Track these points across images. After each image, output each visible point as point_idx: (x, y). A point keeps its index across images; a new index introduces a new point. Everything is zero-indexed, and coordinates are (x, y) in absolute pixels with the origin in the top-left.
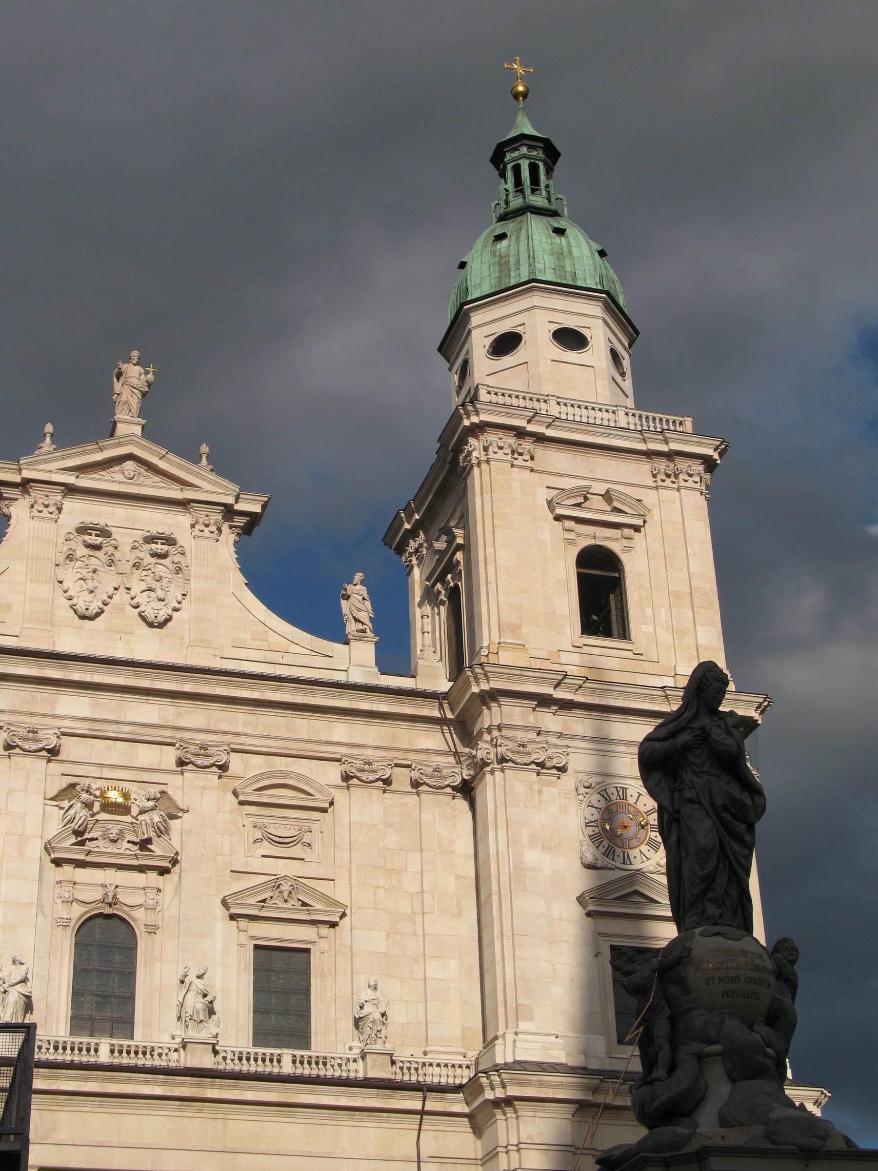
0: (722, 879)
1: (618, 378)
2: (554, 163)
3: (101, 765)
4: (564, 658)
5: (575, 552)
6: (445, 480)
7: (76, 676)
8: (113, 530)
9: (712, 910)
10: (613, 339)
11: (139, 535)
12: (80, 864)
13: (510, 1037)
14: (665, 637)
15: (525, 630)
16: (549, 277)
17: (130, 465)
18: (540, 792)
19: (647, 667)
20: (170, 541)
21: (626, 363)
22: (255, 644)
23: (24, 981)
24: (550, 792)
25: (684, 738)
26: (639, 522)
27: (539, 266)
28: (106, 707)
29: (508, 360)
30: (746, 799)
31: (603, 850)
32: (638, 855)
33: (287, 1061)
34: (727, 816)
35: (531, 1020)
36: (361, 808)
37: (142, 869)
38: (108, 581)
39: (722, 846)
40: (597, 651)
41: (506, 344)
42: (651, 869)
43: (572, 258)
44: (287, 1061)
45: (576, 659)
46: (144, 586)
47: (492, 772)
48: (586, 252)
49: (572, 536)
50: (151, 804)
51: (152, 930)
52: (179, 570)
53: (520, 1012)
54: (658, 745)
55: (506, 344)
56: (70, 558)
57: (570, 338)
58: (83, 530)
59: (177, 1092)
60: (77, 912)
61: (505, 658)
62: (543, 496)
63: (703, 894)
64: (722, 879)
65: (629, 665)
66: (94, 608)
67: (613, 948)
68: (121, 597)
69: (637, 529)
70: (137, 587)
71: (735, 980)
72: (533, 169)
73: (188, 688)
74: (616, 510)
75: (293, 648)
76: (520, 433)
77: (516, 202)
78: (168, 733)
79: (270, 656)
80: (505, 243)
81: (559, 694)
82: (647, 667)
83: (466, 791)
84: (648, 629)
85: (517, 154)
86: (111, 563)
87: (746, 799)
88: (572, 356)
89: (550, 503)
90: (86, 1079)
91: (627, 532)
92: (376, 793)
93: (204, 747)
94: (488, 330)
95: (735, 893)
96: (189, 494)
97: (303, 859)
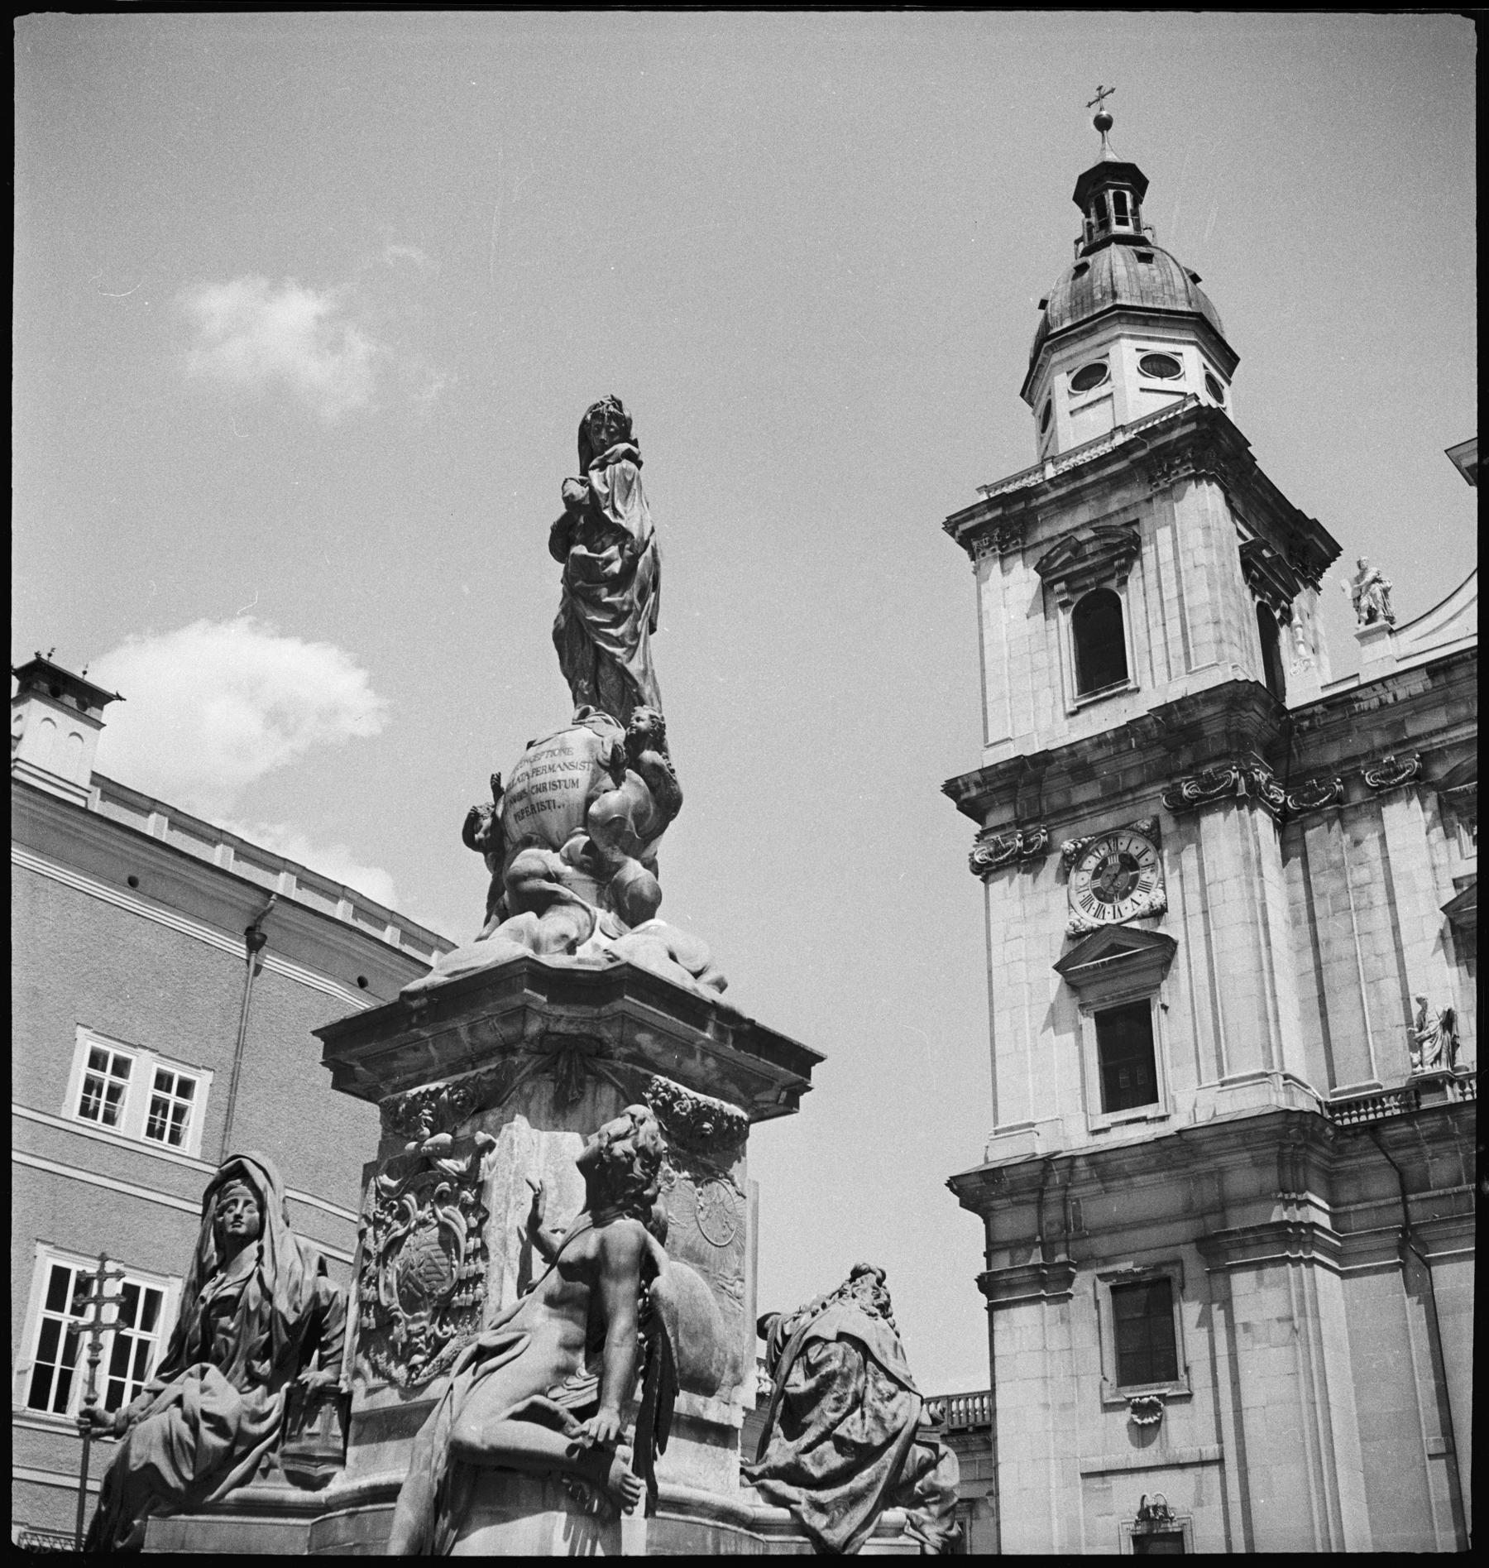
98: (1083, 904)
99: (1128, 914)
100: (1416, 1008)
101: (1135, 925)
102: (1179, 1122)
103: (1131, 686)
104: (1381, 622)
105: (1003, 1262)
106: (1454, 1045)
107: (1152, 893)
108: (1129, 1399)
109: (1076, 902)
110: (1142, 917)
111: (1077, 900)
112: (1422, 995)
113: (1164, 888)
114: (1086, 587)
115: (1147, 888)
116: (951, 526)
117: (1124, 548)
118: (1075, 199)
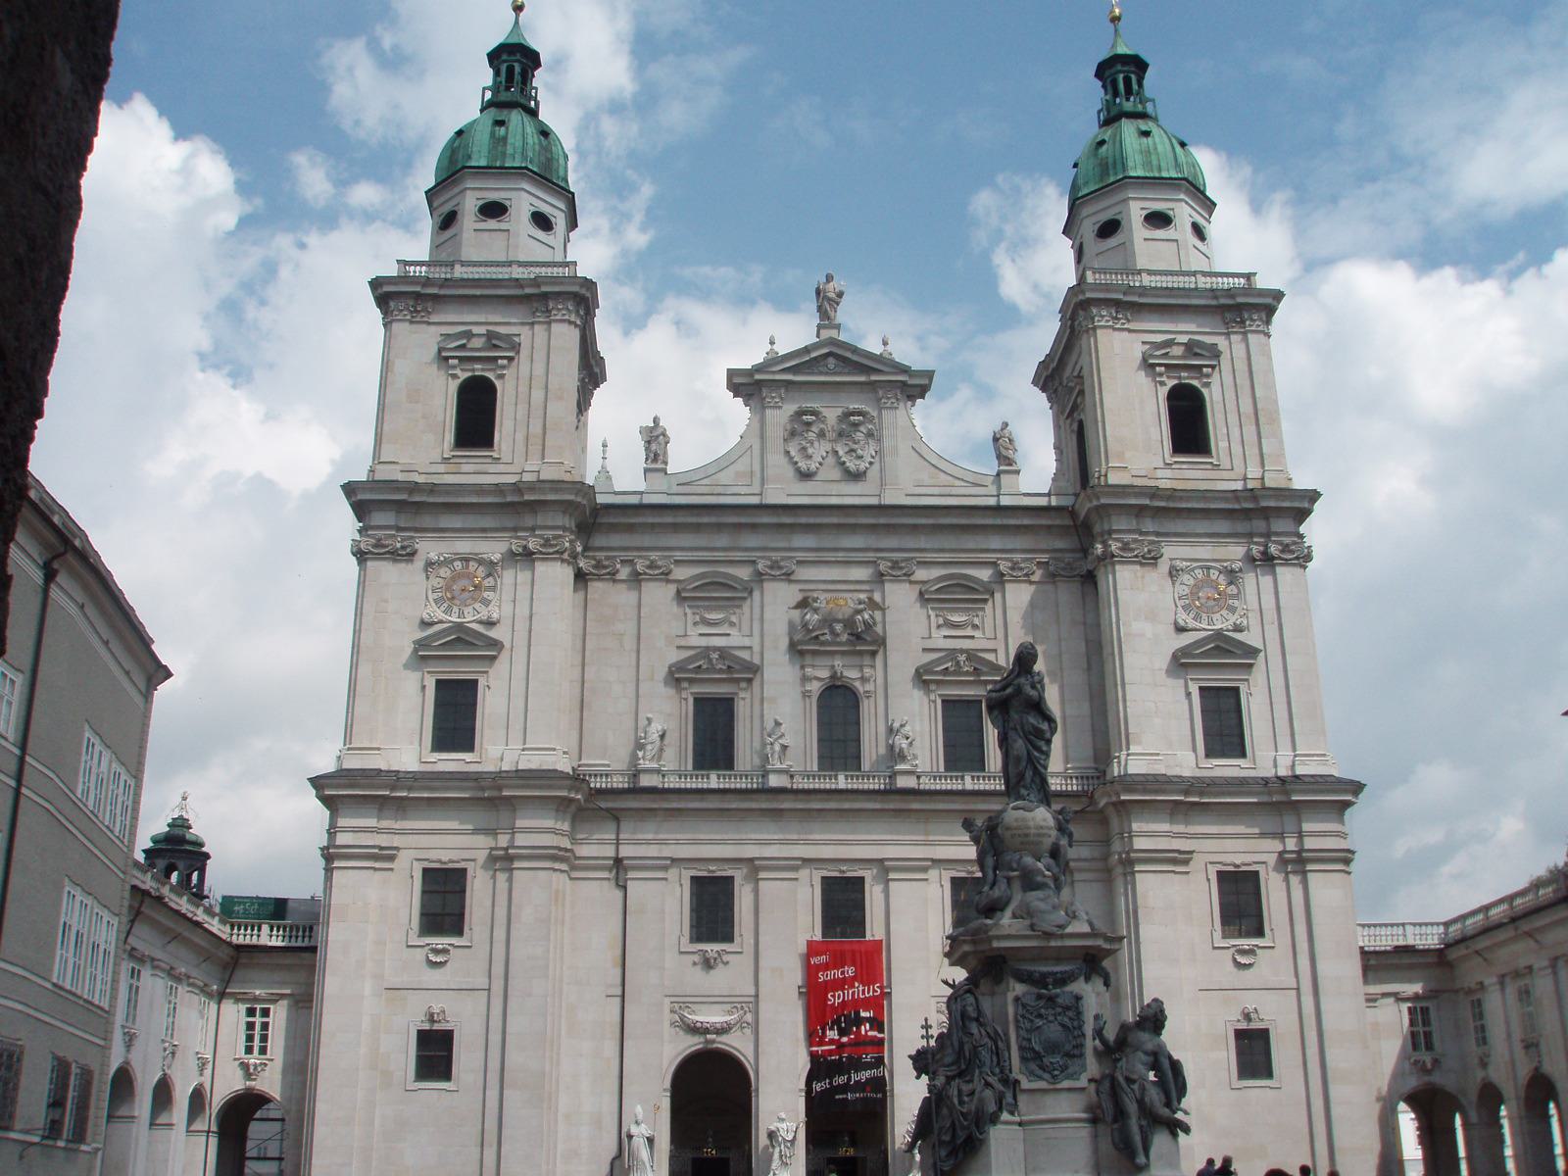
0: (1029, 774)
1: (1199, 244)
2: (1145, 71)
3: (825, 582)
4: (1160, 474)
5: (1163, 392)
6: (1069, 340)
8: (821, 409)
9: (1023, 792)
10: (1194, 214)
11: (839, 412)
12: (815, 653)
14: (1237, 449)
15: (1128, 455)
16: (1140, 173)
18: (1143, 577)
20: (860, 413)
22: (932, 482)
25: (1009, 690)
27: (1130, 164)
28: (828, 541)
29: (1112, 242)
30: (1045, 726)
31: (1192, 615)
32: (1219, 617)
33: (968, 779)
34: (1032, 737)
35: (1139, 743)
37: (861, 653)
38: (819, 450)
39: (1028, 754)
40: (1184, 466)
42: (1230, 628)
43: (1158, 154)
44: (968, 779)
45: (1168, 473)
46: (847, 449)
47: (1105, 566)
48: (1169, 148)
49: (1164, 379)
50: (862, 606)
52: (870, 435)
54: (994, 694)
55: (1109, 229)
56: (793, 434)
58: (800, 413)
59: (891, 806)
60: (815, 687)
61: (1114, 479)
62: (1137, 351)
63: (1019, 782)
64: (1029, 774)
67: (1201, 689)
69: (1213, 367)
71: (1027, 835)
72: (1127, 82)
73: (882, 521)
75: (957, 483)
78: (872, 555)
80: (1105, 147)
83: (1090, 579)
85: (1113, 70)
86: (822, 435)
87: (1045, 726)
88: (1160, 233)
89: (1144, 354)
90: (827, 800)
94: (1094, 219)
95: (1038, 781)
96: (874, 378)
97: (973, 637)
100: (642, 723)
101: (474, 626)
102: (489, 767)
103: (496, 455)
104: (659, 466)
105: (342, 839)
106: (661, 750)
107: (490, 608)
108: (428, 944)
109: (431, 597)
110: (481, 622)
111: (431, 597)
112: (650, 715)
113: (499, 607)
114: (473, 370)
115: (486, 602)
116: (376, 284)
117: (502, 347)
118: (488, 55)
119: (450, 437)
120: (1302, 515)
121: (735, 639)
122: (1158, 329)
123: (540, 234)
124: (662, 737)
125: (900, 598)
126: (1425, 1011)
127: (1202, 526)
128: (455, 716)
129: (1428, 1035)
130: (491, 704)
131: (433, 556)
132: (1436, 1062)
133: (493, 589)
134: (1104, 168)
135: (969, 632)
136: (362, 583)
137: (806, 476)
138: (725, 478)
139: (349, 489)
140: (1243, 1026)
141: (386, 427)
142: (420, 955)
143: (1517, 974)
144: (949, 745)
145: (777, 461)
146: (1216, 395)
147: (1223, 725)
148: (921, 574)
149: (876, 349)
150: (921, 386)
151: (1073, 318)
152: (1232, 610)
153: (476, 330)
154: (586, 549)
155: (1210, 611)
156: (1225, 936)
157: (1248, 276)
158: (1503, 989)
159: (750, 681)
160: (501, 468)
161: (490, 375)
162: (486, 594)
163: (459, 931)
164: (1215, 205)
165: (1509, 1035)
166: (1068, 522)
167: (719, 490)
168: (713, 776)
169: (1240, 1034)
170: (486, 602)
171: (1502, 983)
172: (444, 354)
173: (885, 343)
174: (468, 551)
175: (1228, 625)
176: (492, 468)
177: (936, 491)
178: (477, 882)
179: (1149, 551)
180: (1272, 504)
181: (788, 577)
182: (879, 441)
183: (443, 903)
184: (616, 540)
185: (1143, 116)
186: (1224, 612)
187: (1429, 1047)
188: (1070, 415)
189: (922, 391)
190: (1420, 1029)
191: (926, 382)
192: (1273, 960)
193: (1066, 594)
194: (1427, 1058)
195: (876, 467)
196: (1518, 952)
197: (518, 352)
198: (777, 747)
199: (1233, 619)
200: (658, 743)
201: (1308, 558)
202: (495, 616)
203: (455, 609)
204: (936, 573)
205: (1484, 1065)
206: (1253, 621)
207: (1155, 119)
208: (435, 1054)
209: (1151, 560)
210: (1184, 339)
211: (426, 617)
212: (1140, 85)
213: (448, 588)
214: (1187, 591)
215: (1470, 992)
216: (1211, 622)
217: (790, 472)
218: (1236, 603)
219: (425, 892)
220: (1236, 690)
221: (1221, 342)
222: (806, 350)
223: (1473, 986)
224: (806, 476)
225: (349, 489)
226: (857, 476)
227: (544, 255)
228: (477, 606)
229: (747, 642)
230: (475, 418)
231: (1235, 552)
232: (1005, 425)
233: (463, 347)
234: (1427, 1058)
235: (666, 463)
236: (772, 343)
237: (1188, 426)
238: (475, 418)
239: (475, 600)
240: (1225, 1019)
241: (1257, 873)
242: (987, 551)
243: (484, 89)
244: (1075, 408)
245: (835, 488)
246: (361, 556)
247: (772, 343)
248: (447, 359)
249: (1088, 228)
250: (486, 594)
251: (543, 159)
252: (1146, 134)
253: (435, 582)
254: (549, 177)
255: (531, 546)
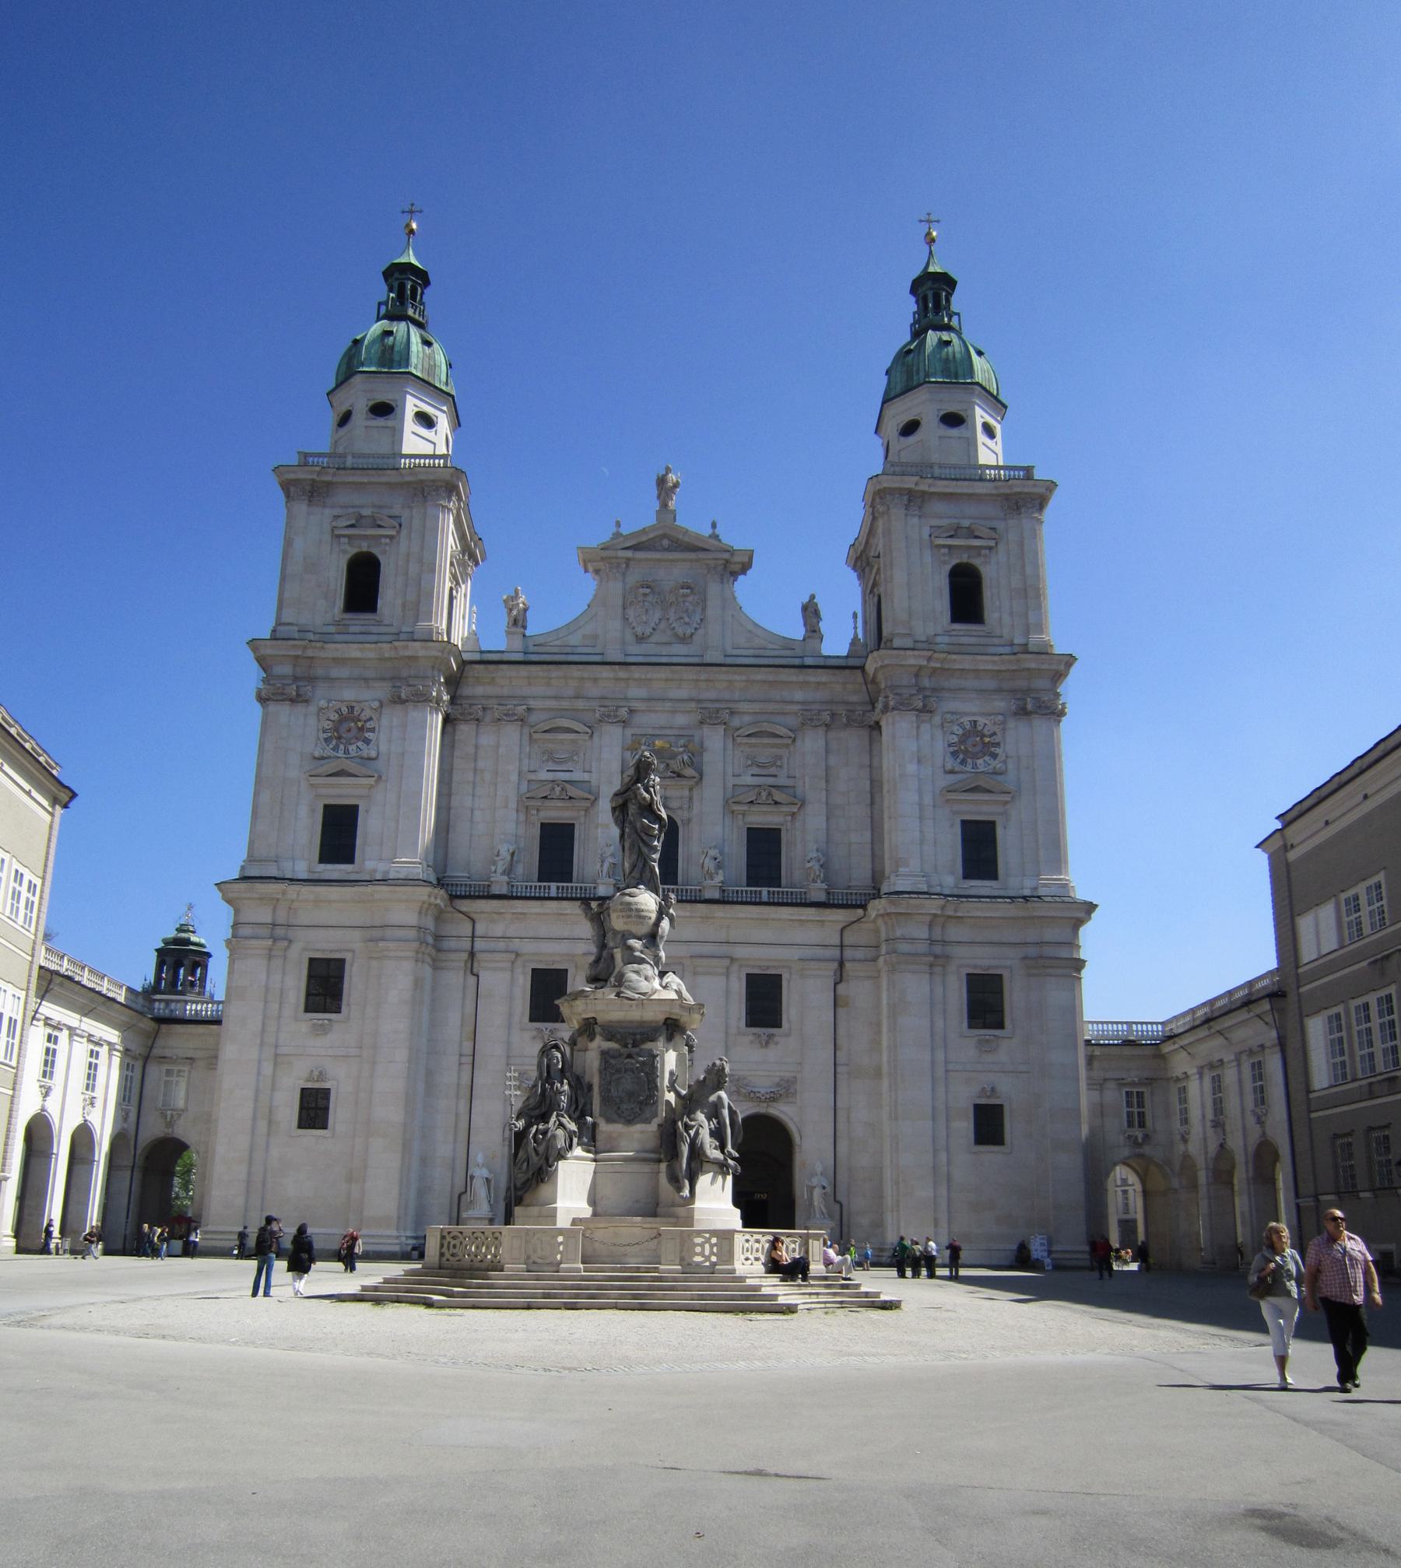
4: (939, 639)
5: (948, 568)
7: (637, 675)
13: (893, 878)
17: (666, 542)
19: (996, 641)
21: (998, 429)
23: (613, 855)
24: (925, 727)
26: (992, 543)
29: (912, 439)
36: (812, 743)
41: (910, 428)
45: (946, 639)
51: (689, 820)
53: (898, 863)
55: (910, 428)
57: (953, 420)
62: (926, 531)
65: (982, 641)
66: (647, 633)
67: (964, 822)
68: (663, 625)
69: (990, 548)
70: (672, 616)
73: (703, 677)
74: (977, 537)
76: (910, 493)
77: (924, 322)
79: (757, 652)
81: (933, 664)
82: (996, 641)
83: (877, 727)
84: (996, 615)
88: (954, 432)
91: (983, 552)
92: (821, 731)
93: (718, 711)
98: (326, 740)
99: (353, 754)
115: (367, 741)
119: (340, 603)
120: (1058, 676)
121: (577, 776)
122: (942, 514)
123: (423, 431)
124: (513, 854)
125: (714, 739)
126: (1140, 1095)
127: (971, 683)
128: (339, 833)
129: (1141, 1115)
130: (369, 827)
131: (323, 703)
132: (1146, 1137)
133: (372, 730)
134: (909, 374)
135: (773, 770)
136: (264, 723)
137: (641, 639)
138: (575, 640)
139: (253, 644)
140: (983, 1101)
141: (287, 595)
142: (304, 1027)
143: (1212, 1066)
144: (751, 865)
145: (615, 626)
146: (991, 573)
147: (979, 850)
148: (736, 722)
149: (706, 531)
150: (743, 564)
151: (873, 506)
152: (994, 756)
153: (366, 512)
154: (453, 700)
155: (975, 756)
156: (970, 1027)
157: (1028, 470)
158: (1201, 1077)
159: (587, 810)
160: (383, 629)
161: (375, 551)
162: (367, 735)
163: (338, 1011)
164: (1005, 407)
165: (1204, 1116)
166: (860, 679)
167: (568, 650)
168: (553, 885)
169: (979, 1109)
170: (367, 741)
171: (1201, 1075)
172: (337, 532)
173: (714, 525)
174: (353, 698)
175: (990, 769)
176: (374, 629)
177: (751, 652)
178: (355, 968)
179: (925, 706)
180: (1033, 666)
181: (625, 723)
182: (704, 609)
183: (325, 987)
184: (480, 690)
185: (948, 328)
186: (987, 758)
187: (1142, 1124)
188: (871, 591)
189: (745, 567)
190: (1136, 1110)
191: (746, 559)
192: (1008, 1046)
193: (853, 739)
194: (1139, 1134)
195: (701, 632)
196: (1212, 1048)
197: (398, 532)
198: (606, 865)
199: (997, 764)
200: (509, 858)
201: (1062, 713)
202: (373, 754)
203: (342, 747)
204: (747, 719)
205: (1185, 1140)
206: (1011, 766)
207: (959, 333)
208: (314, 1109)
209: (926, 710)
210: (966, 523)
211: (317, 754)
212: (948, 300)
213: (336, 730)
214: (956, 739)
215: (1178, 1080)
216: (975, 766)
217: (629, 638)
218: (998, 751)
219: (310, 977)
220: (992, 824)
221: (1000, 526)
222: (644, 531)
223: (1180, 1075)
224: (641, 639)
225: (253, 644)
226: (684, 640)
227: (428, 449)
228: (360, 744)
229: (586, 777)
230: (362, 585)
231: (1000, 704)
232: (813, 597)
233: (352, 526)
234: (1139, 1134)
235: (525, 627)
236: (618, 524)
237: (966, 597)
238: (362, 585)
239: (358, 739)
240: (965, 1096)
241: (1000, 976)
242: (791, 702)
243: (380, 304)
244: (875, 584)
245: (665, 650)
246: (262, 699)
247: (618, 524)
248: (339, 536)
249: (892, 426)
250: (367, 735)
251: (426, 365)
252: (948, 343)
253: (327, 725)
254: (431, 380)
255: (403, 696)
